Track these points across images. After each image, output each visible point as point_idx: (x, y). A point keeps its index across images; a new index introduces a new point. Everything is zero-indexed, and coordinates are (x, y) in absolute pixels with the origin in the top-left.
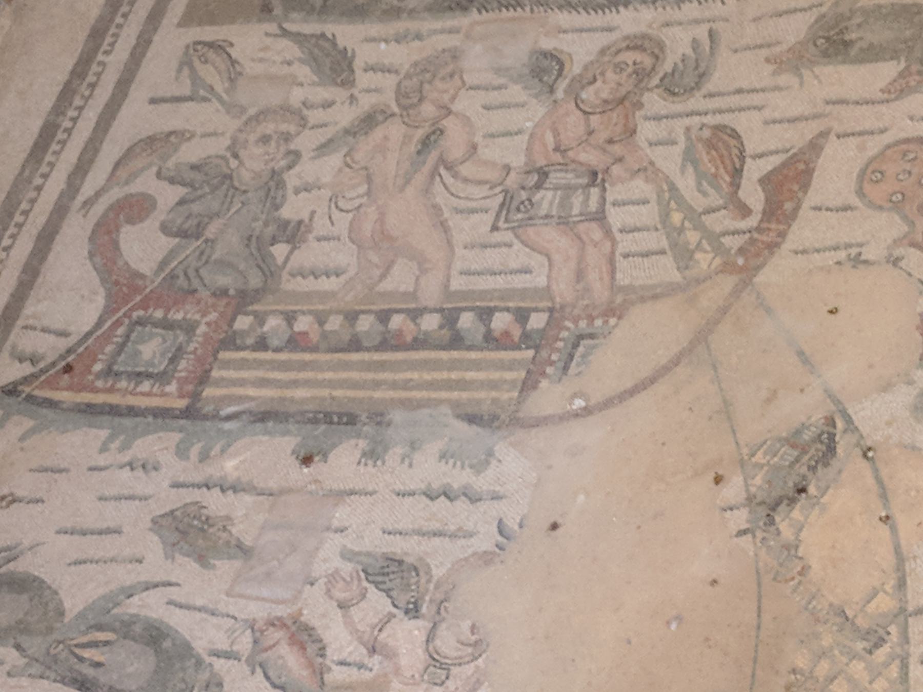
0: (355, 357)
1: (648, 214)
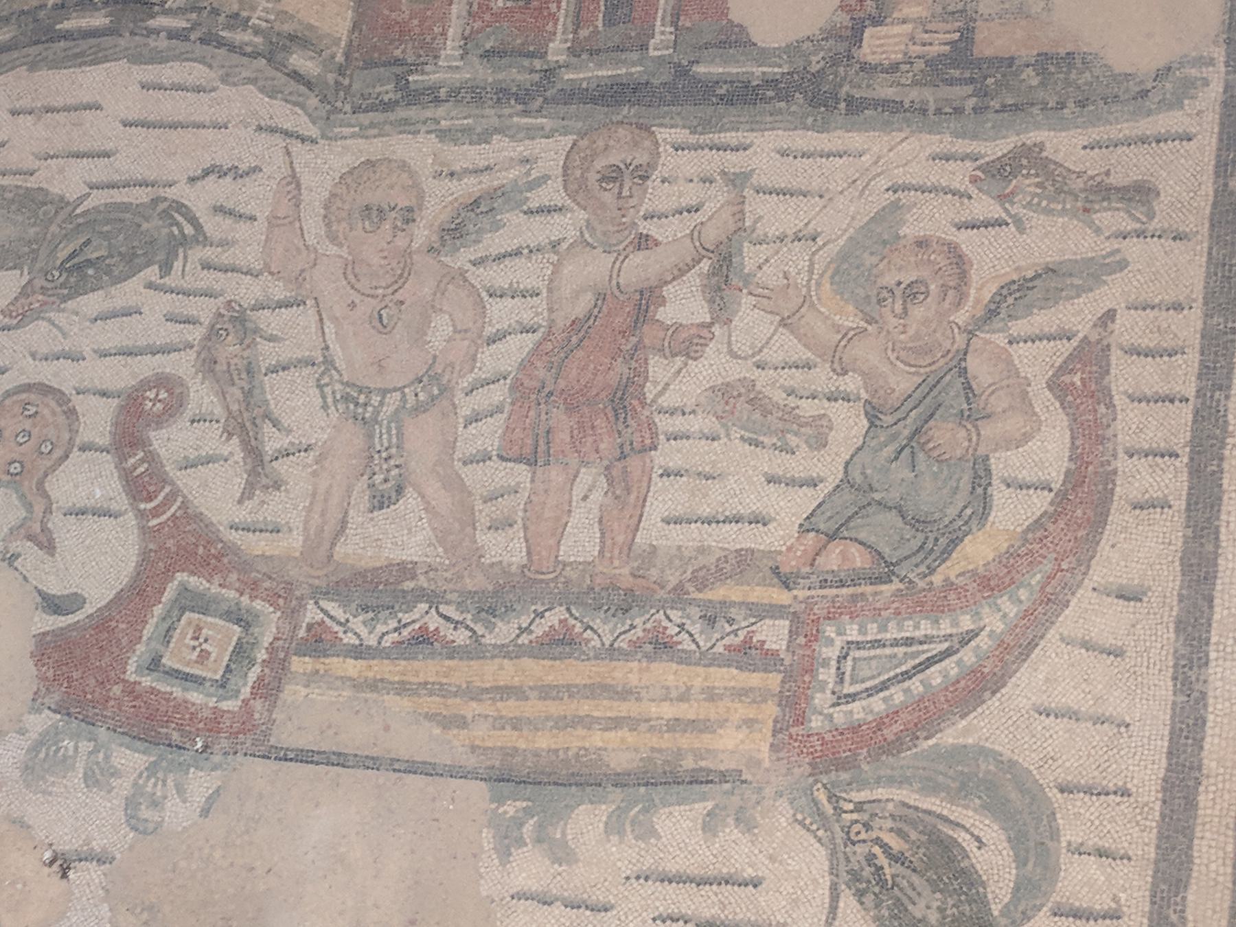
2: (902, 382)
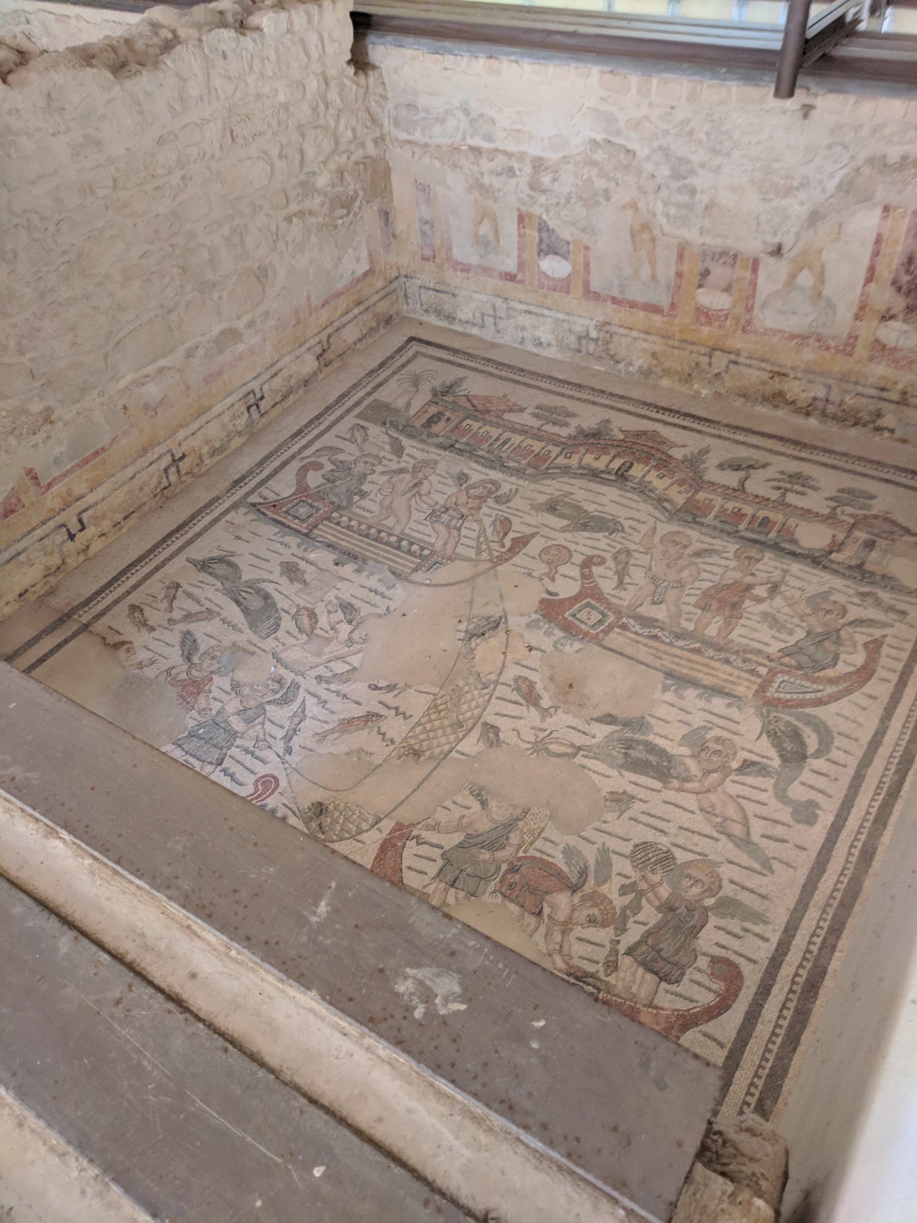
1: (474, 535)
2: (819, 629)
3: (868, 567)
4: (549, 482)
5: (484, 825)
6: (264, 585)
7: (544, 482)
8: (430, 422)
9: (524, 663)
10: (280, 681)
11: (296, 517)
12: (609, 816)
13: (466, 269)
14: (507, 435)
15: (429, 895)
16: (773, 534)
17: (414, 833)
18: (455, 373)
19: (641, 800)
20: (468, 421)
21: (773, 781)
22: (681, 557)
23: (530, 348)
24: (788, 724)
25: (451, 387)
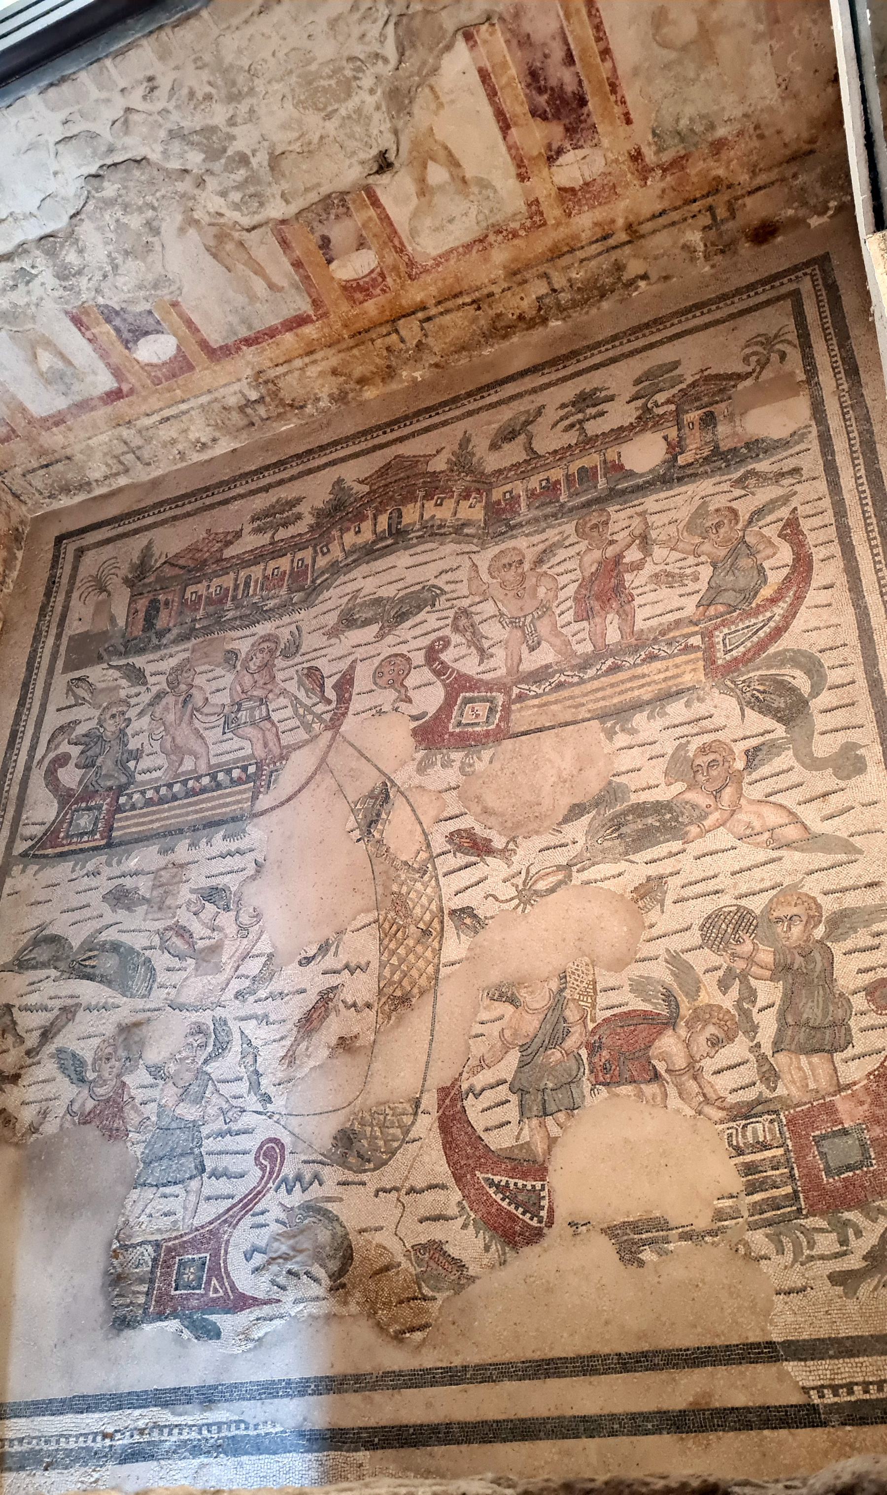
0: (176, 803)
1: (289, 712)
2: (722, 552)
3: (724, 446)
4: (326, 595)
5: (531, 1024)
6: (104, 936)
7: (321, 598)
8: (149, 622)
9: (446, 814)
10: (199, 1030)
11: (82, 835)
12: (653, 916)
13: (58, 420)
14: (243, 574)
15: (528, 1143)
16: (602, 483)
17: (465, 1086)
18: (135, 546)
19: (671, 874)
20: (191, 589)
21: (791, 752)
22: (523, 576)
23: (196, 457)
24: (762, 680)
25: (143, 563)
